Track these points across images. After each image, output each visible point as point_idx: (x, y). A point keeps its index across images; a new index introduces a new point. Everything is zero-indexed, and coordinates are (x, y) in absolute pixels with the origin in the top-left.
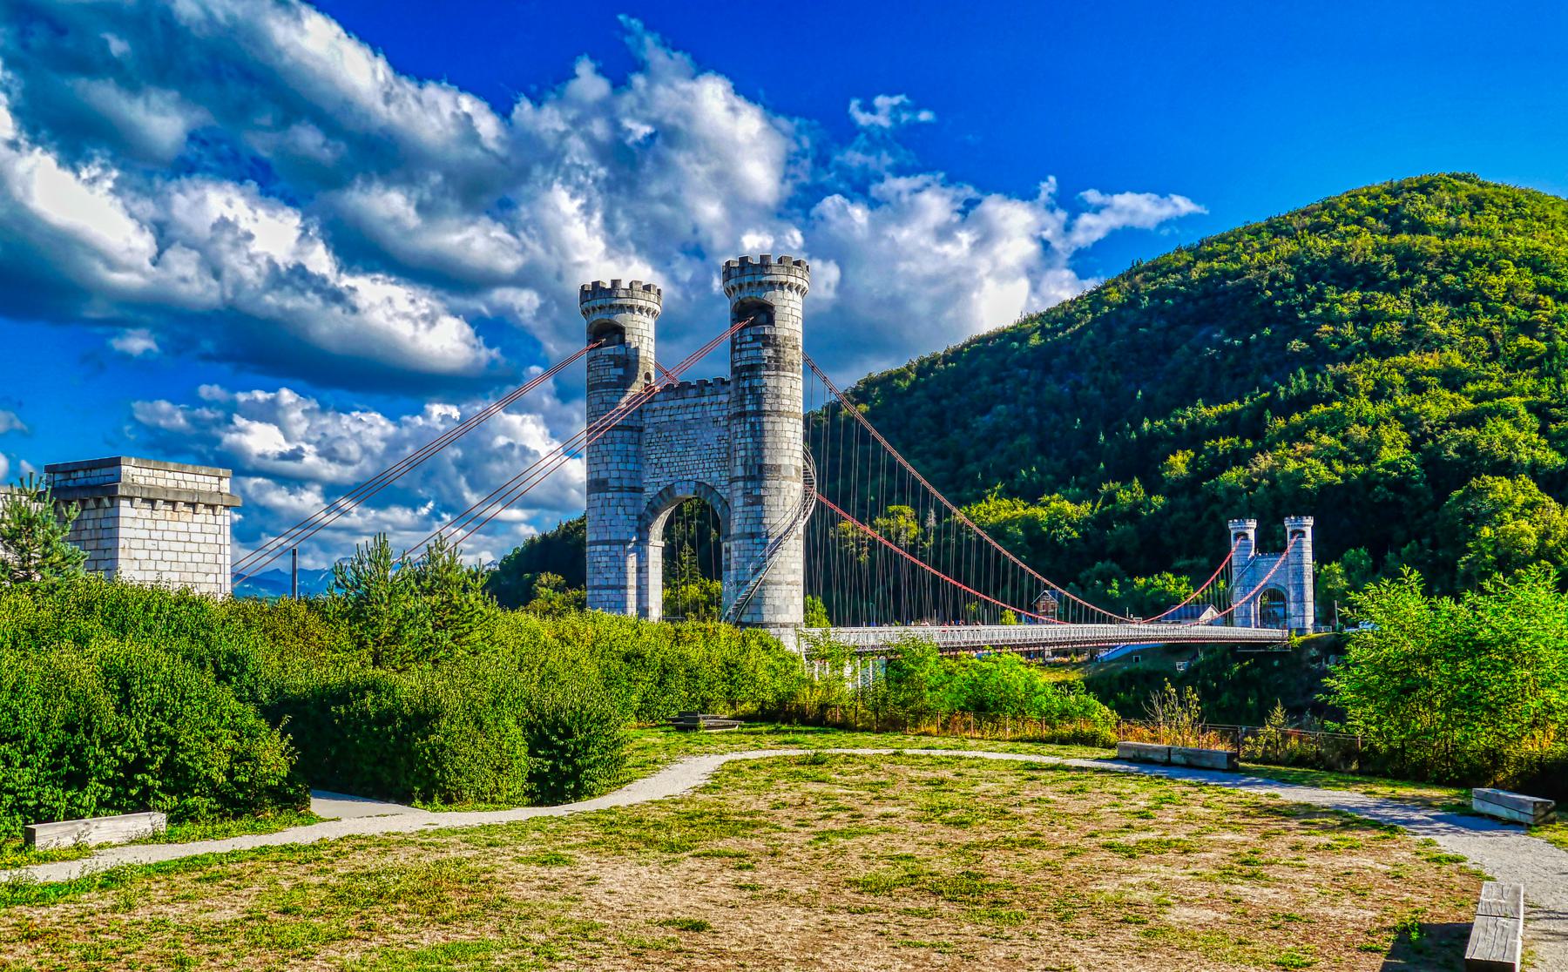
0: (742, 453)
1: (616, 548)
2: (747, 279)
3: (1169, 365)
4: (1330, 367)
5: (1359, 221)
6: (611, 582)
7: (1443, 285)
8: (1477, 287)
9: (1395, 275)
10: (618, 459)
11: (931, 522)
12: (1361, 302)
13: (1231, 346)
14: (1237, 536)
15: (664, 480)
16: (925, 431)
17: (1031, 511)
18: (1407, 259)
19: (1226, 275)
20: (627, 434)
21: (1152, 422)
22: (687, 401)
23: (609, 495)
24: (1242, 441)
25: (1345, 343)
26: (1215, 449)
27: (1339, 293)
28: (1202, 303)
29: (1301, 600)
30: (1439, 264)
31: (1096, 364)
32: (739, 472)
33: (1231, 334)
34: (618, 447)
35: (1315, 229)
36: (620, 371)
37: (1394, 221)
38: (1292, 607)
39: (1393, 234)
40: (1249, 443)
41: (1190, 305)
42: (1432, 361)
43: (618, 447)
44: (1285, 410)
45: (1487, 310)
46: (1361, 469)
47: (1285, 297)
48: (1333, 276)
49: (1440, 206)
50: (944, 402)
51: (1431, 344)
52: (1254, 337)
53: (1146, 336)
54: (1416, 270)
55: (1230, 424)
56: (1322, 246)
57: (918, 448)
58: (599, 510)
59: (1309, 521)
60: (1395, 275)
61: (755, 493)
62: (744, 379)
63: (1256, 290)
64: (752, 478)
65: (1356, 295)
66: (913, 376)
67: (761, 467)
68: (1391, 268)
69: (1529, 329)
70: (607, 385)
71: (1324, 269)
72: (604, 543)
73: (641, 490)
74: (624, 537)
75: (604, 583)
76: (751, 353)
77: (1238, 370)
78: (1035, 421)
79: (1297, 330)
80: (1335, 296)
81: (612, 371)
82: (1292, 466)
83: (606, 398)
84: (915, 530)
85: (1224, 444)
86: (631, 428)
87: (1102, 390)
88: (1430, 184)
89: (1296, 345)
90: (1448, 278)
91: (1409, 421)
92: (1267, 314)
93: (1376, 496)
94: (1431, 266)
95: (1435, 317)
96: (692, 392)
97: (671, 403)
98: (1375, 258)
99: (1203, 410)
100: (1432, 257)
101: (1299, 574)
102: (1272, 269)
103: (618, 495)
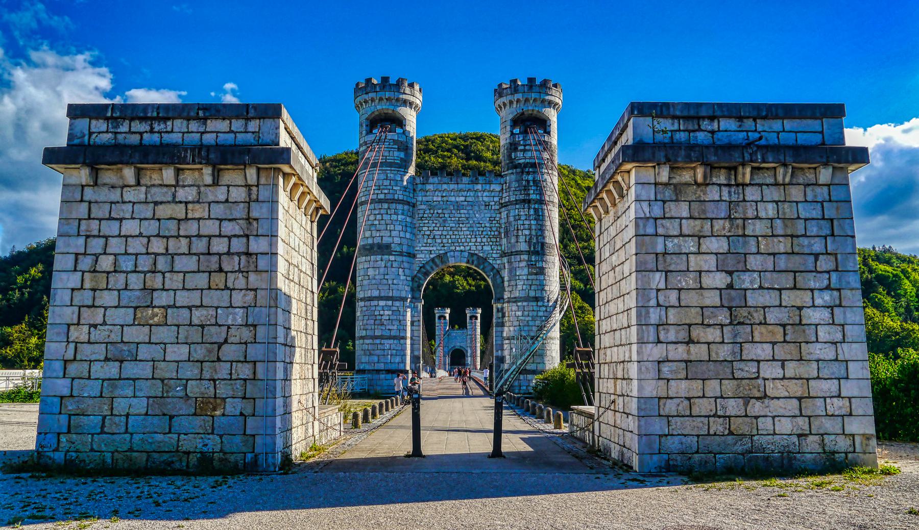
1: (397, 303)
5: (449, 150)
6: (393, 333)
10: (400, 228)
14: (440, 318)
15: (436, 250)
20: (406, 207)
21: (348, 248)
22: (460, 186)
23: (392, 258)
29: (474, 356)
32: (523, 246)
34: (400, 217)
37: (468, 153)
38: (469, 360)
39: (468, 159)
43: (400, 217)
49: (488, 149)
58: (382, 270)
59: (480, 311)
61: (539, 265)
62: (528, 173)
64: (536, 253)
67: (543, 244)
70: (391, 165)
72: (387, 298)
73: (414, 256)
74: (403, 294)
75: (387, 333)
81: (396, 154)
83: (391, 176)
86: (408, 203)
88: (481, 136)
97: (445, 186)
101: (473, 340)
103: (399, 259)
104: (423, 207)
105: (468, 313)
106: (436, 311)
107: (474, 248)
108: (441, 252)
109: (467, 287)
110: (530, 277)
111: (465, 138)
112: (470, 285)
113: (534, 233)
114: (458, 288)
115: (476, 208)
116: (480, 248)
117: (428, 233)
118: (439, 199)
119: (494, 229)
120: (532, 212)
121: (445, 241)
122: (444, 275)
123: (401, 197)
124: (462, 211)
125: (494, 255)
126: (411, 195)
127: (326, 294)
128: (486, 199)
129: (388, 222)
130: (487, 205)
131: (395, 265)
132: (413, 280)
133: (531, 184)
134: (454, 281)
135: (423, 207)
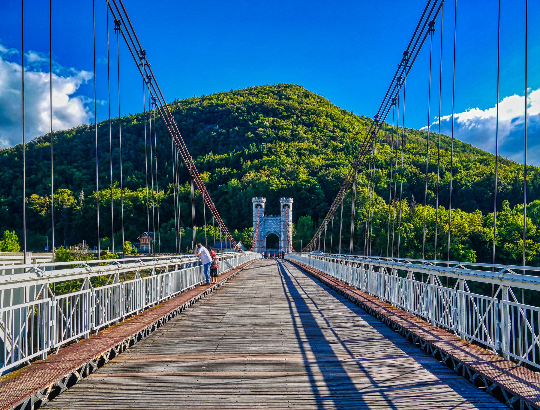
3: (195, 138)
4: (264, 145)
7: (302, 119)
8: (314, 122)
9: (285, 114)
11: (82, 197)
12: (273, 121)
13: (221, 134)
16: (79, 157)
17: (135, 194)
18: (288, 109)
19: (218, 105)
24: (232, 170)
25: (268, 136)
26: (221, 172)
27: (264, 117)
28: (208, 115)
30: (300, 112)
31: (162, 134)
33: (221, 127)
35: (251, 94)
37: (280, 96)
38: (282, 243)
40: (235, 171)
41: (203, 115)
42: (305, 145)
44: (252, 157)
45: (318, 130)
46: (293, 182)
47: (243, 116)
48: (261, 111)
49: (295, 94)
50: (89, 145)
51: (301, 140)
52: (231, 130)
53: (185, 125)
54: (292, 113)
55: (226, 163)
56: (257, 100)
57: (76, 164)
59: (292, 200)
60: (285, 114)
63: (231, 112)
65: (271, 119)
66: (74, 133)
68: (282, 111)
69: (334, 138)
71: (258, 108)
77: (225, 142)
78: (134, 156)
79: (249, 129)
80: (262, 118)
82: (264, 178)
84: (72, 200)
85: (224, 170)
87: (165, 145)
88: (290, 86)
89: (249, 134)
90: (303, 117)
91: (308, 166)
92: (236, 122)
93: (302, 194)
94: (297, 112)
95: (301, 130)
98: (277, 106)
99: (213, 156)
100: (297, 109)
101: (286, 226)
102: (237, 105)
105: (282, 202)
106: (253, 201)
109: (280, 185)
111: (279, 87)
112: (283, 184)
114: (272, 186)
122: (261, 176)
127: (168, 192)
134: (269, 180)
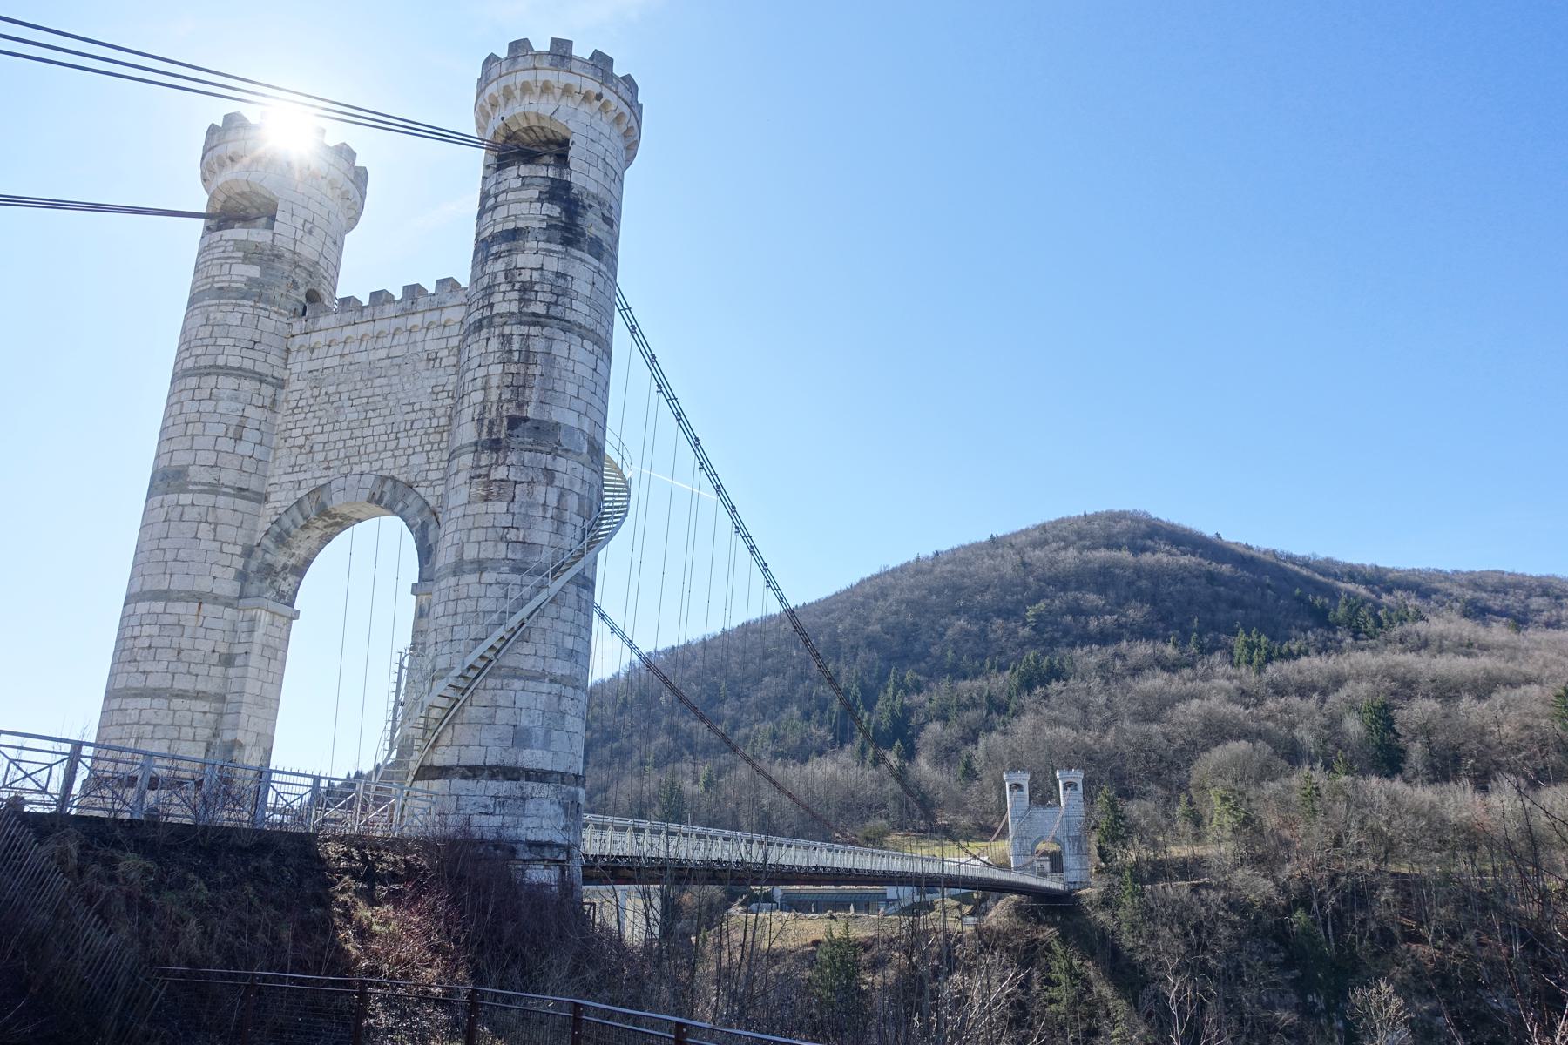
0: (478, 397)
1: (179, 607)
2: (521, 77)
6: (153, 682)
15: (311, 478)
20: (249, 385)
22: (379, 326)
23: (185, 499)
32: (467, 433)
36: (254, 271)
62: (497, 256)
73: (263, 498)
76: (515, 209)
86: (261, 379)
96: (390, 310)
97: (348, 331)
103: (206, 500)
104: (301, 385)
107: (389, 463)
108: (321, 482)
110: (471, 510)
113: (494, 396)
115: (409, 368)
116: (402, 461)
117: (301, 441)
118: (336, 361)
119: (439, 412)
120: (495, 344)
121: (331, 455)
123: (234, 362)
124: (377, 382)
125: (431, 476)
126: (280, 362)
128: (431, 346)
129: (192, 417)
130: (432, 359)
131: (191, 513)
132: (248, 553)
133: (501, 278)
135: (301, 385)
